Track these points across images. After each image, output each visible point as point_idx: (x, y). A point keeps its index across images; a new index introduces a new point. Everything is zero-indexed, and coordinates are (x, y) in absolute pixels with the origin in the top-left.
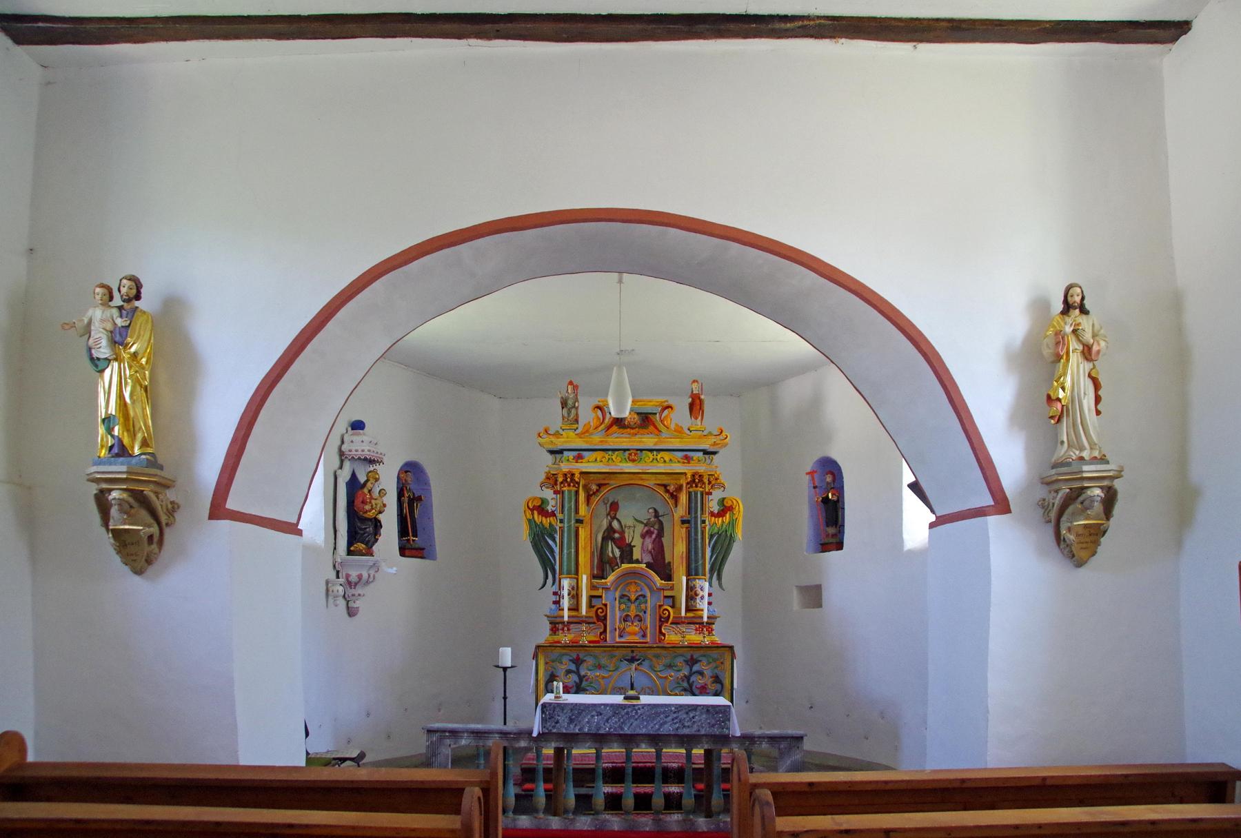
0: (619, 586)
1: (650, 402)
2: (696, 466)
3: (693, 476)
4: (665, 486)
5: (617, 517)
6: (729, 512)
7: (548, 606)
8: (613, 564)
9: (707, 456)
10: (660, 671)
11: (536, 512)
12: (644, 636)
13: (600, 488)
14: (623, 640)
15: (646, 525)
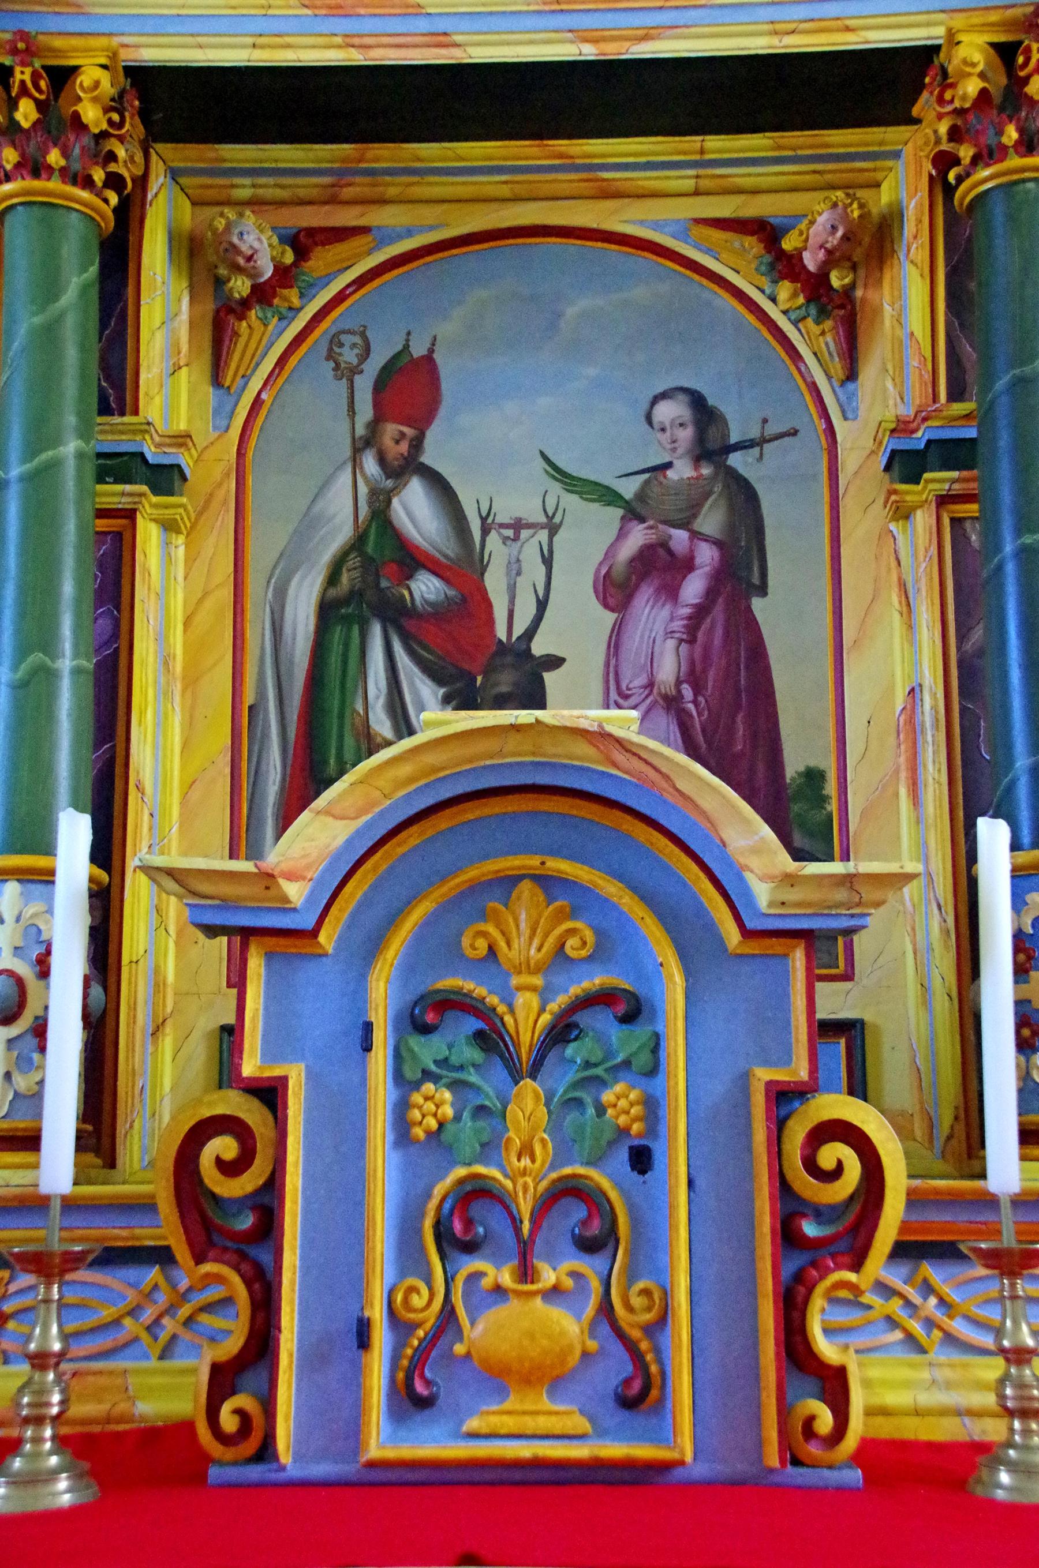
0: (393, 920)
13: (302, 253)
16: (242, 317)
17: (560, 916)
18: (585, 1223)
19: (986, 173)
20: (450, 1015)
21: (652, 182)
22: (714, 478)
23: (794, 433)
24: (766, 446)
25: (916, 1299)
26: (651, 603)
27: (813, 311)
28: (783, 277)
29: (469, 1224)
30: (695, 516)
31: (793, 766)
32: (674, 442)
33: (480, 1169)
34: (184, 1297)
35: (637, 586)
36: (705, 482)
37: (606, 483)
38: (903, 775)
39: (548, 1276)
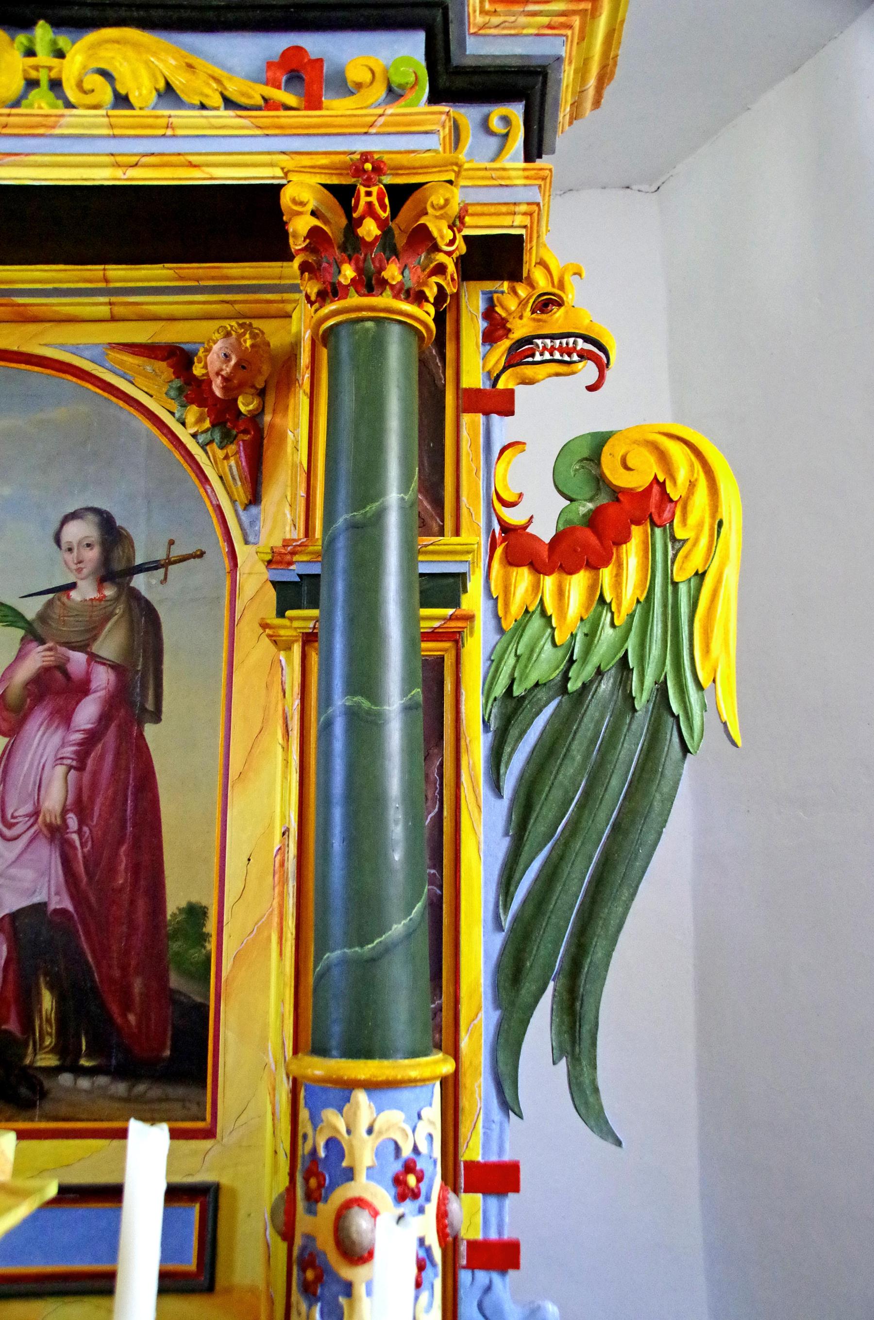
6: (636, 531)
21: (67, 308)
22: (116, 599)
23: (201, 555)
24: (170, 567)
26: (42, 729)
27: (217, 436)
28: (192, 402)
30: (95, 638)
32: (80, 562)
35: (31, 709)
36: (109, 603)
37: (9, 602)
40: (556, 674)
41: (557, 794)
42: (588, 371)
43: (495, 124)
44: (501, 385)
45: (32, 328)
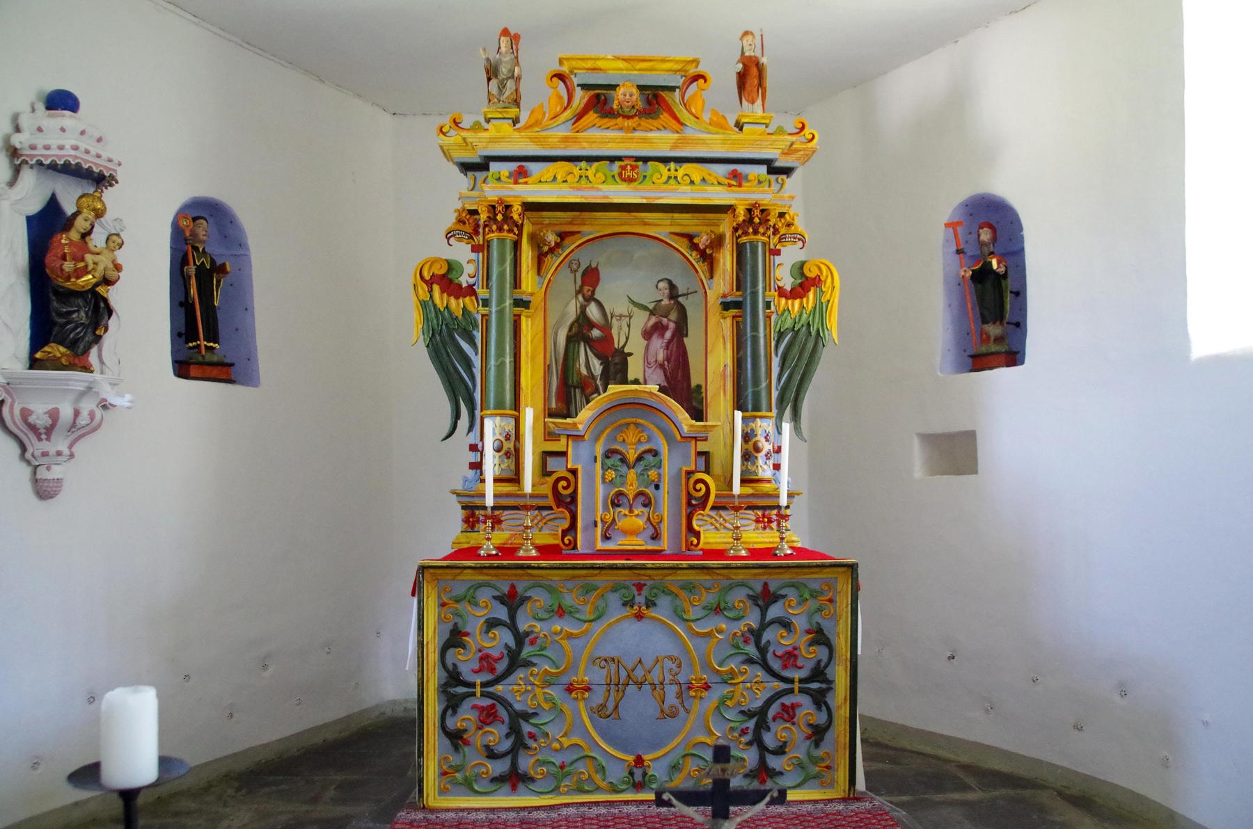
0: (602, 432)
1: (663, 61)
2: (754, 192)
3: (749, 211)
4: (690, 237)
5: (596, 297)
6: (812, 288)
7: (460, 475)
8: (588, 388)
9: (773, 177)
10: (693, 621)
11: (436, 288)
12: (656, 537)
14: (610, 546)
15: (652, 313)
16: (546, 257)
17: (640, 432)
18: (644, 501)
19: (745, 238)
20: (614, 455)
22: (674, 303)
25: (718, 519)
27: (702, 259)
29: (618, 501)
31: (694, 383)
33: (621, 489)
34: (544, 518)
35: (653, 334)
37: (644, 304)
38: (722, 387)
39: (636, 512)
40: (792, 326)
41: (792, 356)
42: (800, 244)
43: (780, 181)
44: (777, 247)
45: (647, 226)
